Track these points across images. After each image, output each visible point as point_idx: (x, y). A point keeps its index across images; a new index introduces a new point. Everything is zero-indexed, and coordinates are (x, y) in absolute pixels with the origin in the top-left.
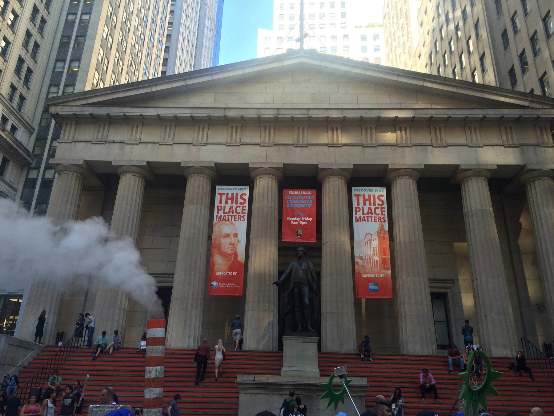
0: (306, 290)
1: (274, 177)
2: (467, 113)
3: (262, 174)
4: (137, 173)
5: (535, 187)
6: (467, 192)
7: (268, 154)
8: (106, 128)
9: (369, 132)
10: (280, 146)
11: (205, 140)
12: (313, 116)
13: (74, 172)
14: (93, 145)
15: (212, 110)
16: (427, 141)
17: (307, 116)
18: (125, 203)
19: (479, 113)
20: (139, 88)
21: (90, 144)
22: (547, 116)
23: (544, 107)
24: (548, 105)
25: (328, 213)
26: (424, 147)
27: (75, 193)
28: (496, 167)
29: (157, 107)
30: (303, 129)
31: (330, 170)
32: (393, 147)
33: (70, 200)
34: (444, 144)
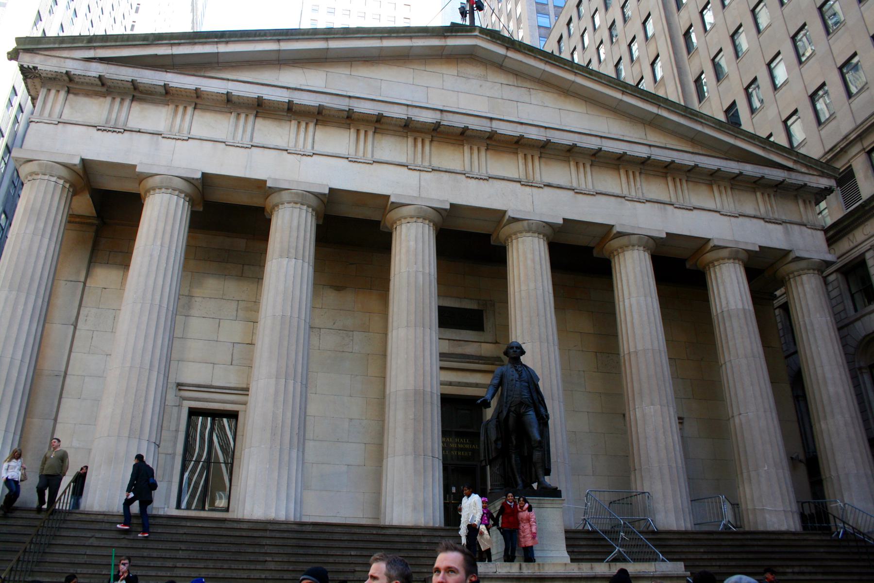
0: (531, 416)
1: (431, 224)
2: (718, 164)
3: (412, 217)
4: (181, 191)
5: (802, 284)
6: (719, 281)
7: (422, 183)
8: (127, 103)
9: (582, 169)
10: (443, 174)
11: (309, 147)
12: (499, 131)
13: (59, 178)
14: (100, 132)
15: (328, 97)
16: (664, 197)
17: (489, 130)
18: (159, 243)
19: (733, 167)
20: (195, 43)
21: (95, 129)
22: (815, 185)
23: (811, 172)
24: (816, 170)
25: (524, 294)
26: (662, 205)
27: (59, 218)
28: (757, 249)
29: (228, 80)
30: (479, 149)
31: (525, 223)
32: (619, 199)
33: (49, 230)
34: (687, 204)
